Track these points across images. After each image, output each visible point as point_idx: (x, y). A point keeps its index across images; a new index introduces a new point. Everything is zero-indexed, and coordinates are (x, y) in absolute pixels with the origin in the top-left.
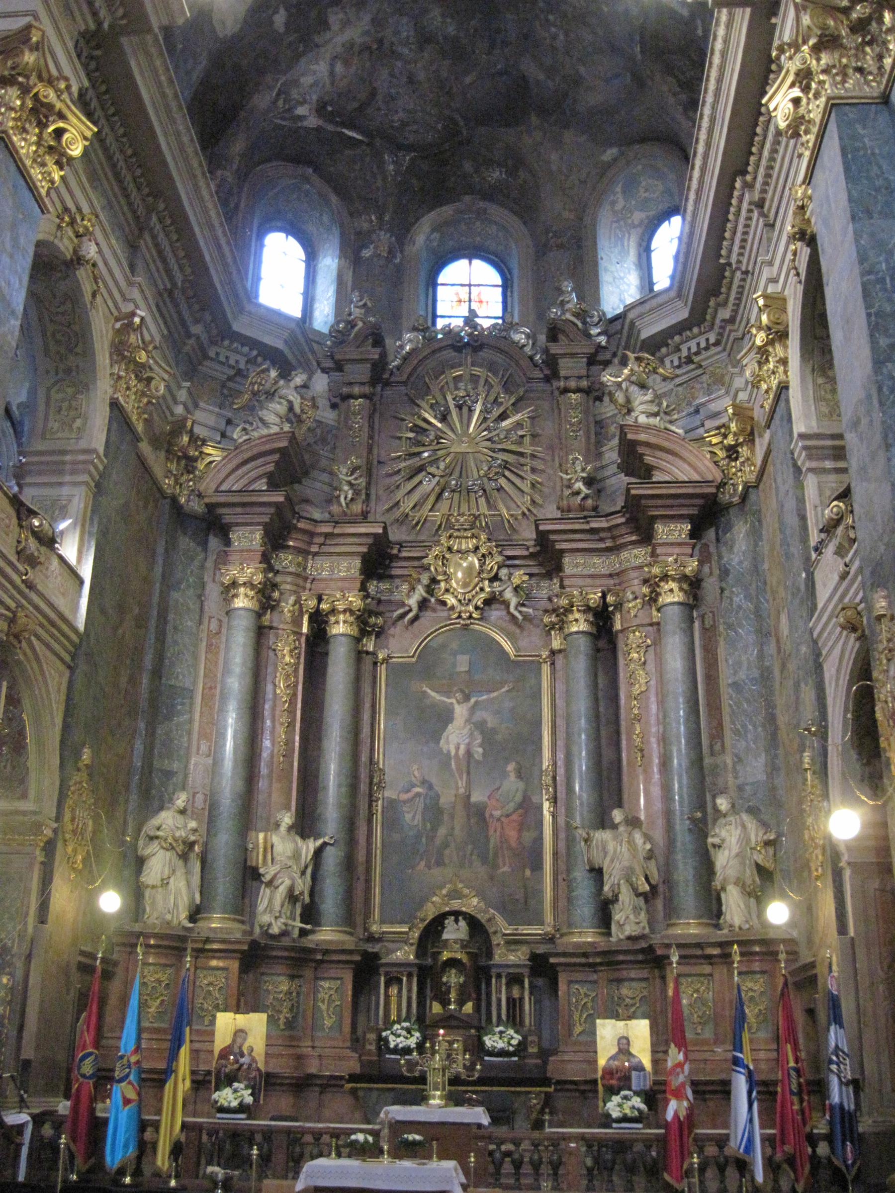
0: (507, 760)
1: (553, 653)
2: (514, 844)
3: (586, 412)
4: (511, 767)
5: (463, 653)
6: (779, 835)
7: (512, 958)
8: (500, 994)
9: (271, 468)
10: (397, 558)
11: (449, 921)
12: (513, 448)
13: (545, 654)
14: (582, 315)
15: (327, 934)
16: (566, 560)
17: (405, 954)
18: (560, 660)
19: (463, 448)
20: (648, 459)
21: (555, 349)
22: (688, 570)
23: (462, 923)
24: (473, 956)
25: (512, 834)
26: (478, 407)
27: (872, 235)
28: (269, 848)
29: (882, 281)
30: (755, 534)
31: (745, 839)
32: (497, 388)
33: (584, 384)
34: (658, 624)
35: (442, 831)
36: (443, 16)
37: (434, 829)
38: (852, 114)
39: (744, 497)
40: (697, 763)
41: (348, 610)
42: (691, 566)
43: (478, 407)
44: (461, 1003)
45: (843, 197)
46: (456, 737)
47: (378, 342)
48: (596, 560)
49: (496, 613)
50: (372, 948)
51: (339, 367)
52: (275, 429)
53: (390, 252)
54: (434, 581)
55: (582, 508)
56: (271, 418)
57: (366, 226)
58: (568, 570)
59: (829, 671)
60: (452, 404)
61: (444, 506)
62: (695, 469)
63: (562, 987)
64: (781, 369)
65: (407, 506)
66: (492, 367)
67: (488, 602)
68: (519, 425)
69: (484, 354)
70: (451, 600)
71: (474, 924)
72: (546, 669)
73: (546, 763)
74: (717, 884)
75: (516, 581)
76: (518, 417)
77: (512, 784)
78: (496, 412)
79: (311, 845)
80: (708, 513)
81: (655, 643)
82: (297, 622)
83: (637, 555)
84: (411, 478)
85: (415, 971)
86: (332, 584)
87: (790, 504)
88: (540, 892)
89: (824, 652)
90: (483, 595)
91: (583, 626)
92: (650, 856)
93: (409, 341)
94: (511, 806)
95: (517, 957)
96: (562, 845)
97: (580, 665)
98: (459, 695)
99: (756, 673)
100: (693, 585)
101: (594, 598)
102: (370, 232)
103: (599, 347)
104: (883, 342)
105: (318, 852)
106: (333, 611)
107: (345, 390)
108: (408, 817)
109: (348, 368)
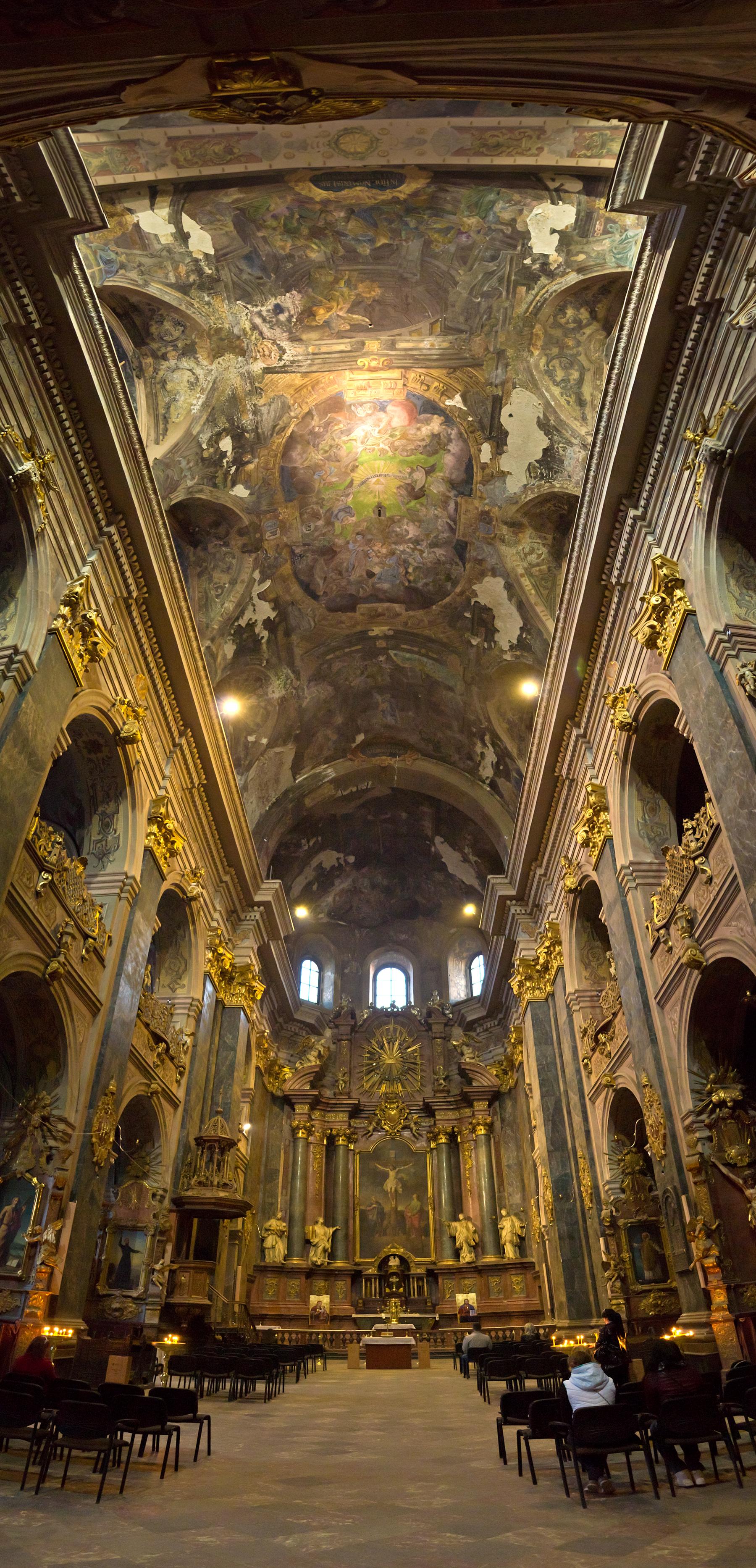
1: (432, 1149)
7: (419, 1271)
11: (391, 1258)
17: (372, 1271)
18: (435, 1152)
19: (390, 1061)
21: (430, 1021)
24: (403, 1271)
25: (416, 1223)
26: (397, 1043)
32: (405, 1035)
38: (536, 1005)
42: (489, 1120)
43: (397, 1043)
44: (398, 1288)
47: (353, 1016)
48: (450, 1113)
49: (406, 1133)
50: (360, 1268)
54: (380, 1120)
61: (384, 1086)
65: (367, 1086)
66: (403, 1025)
68: (415, 1051)
69: (399, 1018)
70: (387, 1128)
71: (402, 1259)
73: (429, 1195)
83: (467, 1112)
88: (429, 1245)
91: (443, 1140)
95: (421, 1271)
101: (449, 1130)
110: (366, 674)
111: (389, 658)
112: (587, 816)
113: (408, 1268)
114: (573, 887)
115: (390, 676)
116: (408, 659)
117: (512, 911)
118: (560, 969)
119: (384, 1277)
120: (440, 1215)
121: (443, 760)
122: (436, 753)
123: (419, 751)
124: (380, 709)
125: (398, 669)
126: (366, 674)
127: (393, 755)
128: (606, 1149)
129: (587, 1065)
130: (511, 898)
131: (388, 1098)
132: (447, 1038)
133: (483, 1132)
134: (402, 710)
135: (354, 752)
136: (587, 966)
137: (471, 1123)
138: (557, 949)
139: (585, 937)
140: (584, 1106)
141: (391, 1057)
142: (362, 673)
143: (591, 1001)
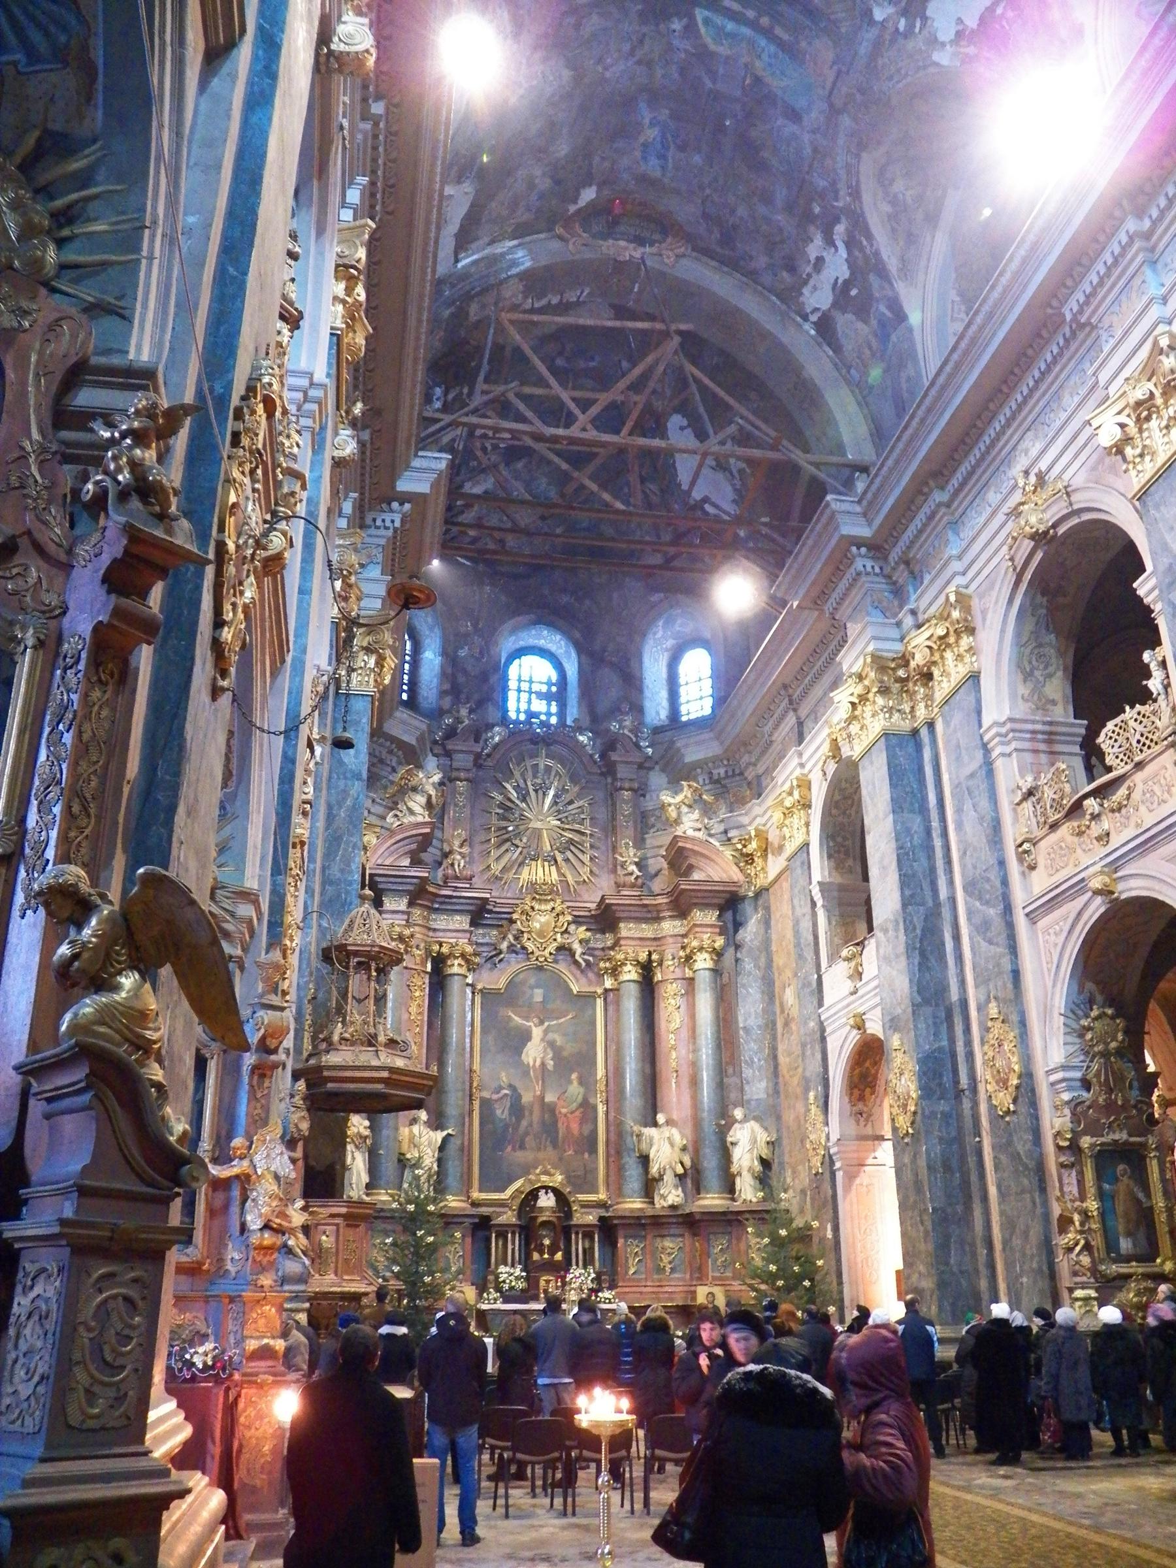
0: (572, 1071)
1: (606, 990)
2: (576, 1132)
3: (636, 806)
4: (574, 1076)
5: (538, 987)
6: (779, 1139)
8: (579, 1245)
9: (414, 846)
10: (490, 912)
11: (542, 1193)
12: (577, 827)
13: (600, 991)
14: (636, 730)
15: (453, 1202)
16: (622, 925)
17: (508, 1217)
19: (538, 825)
20: (693, 861)
21: (614, 757)
22: (717, 945)
23: (551, 1195)
25: (575, 1127)
26: (552, 793)
27: (903, 823)
28: (412, 1137)
29: (907, 854)
30: (767, 923)
31: (754, 1141)
33: (636, 785)
34: (692, 979)
35: (524, 1123)
36: (549, 484)
37: (519, 1120)
39: (758, 895)
40: (720, 1086)
41: (463, 956)
42: (720, 942)
43: (552, 793)
45: (888, 796)
46: (534, 1053)
51: (448, 754)
52: (420, 819)
53: (481, 652)
55: (633, 886)
56: (417, 809)
57: (463, 630)
58: (624, 933)
59: (833, 1044)
60: (531, 788)
61: (526, 870)
62: (725, 871)
63: (621, 1242)
64: (804, 829)
65: (496, 868)
67: (559, 949)
70: (530, 946)
72: (600, 1003)
73: (600, 1072)
74: (734, 1169)
75: (582, 936)
76: (581, 803)
77: (575, 1090)
78: (566, 798)
79: (439, 1136)
80: (730, 905)
81: (687, 993)
82: (424, 964)
84: (499, 846)
85: (517, 1230)
86: (449, 934)
87: (806, 924)
88: (597, 1169)
89: (828, 1030)
90: (555, 944)
92: (684, 1149)
93: (497, 735)
94: (575, 1105)
95: (591, 1218)
96: (613, 1137)
97: (631, 1005)
98: (536, 1020)
99: (760, 1022)
100: (718, 954)
101: (643, 957)
102: (467, 635)
103: (648, 758)
104: (907, 893)
105: (445, 1140)
106: (451, 955)
107: (454, 774)
108: (498, 1112)
109: (458, 757)
110: (639, 54)
111: (690, 29)
112: (1139, 394)
113: (569, 1215)
114: (1042, 528)
115: (682, 71)
116: (732, 36)
117: (859, 564)
118: (974, 678)
119: (528, 1229)
120: (620, 1111)
121: (733, 263)
122: (725, 247)
123: (689, 238)
124: (642, 139)
125: (704, 55)
126: (639, 54)
127: (640, 241)
128: (1060, 1000)
129: (1026, 852)
130: (858, 543)
131: (538, 892)
132: (641, 792)
133: (709, 964)
134: (682, 148)
135: (568, 222)
136: (1027, 676)
137: (683, 948)
138: (966, 641)
139: (1029, 626)
140: (1010, 926)
141: (542, 819)
142: (632, 53)
143: (1032, 740)
